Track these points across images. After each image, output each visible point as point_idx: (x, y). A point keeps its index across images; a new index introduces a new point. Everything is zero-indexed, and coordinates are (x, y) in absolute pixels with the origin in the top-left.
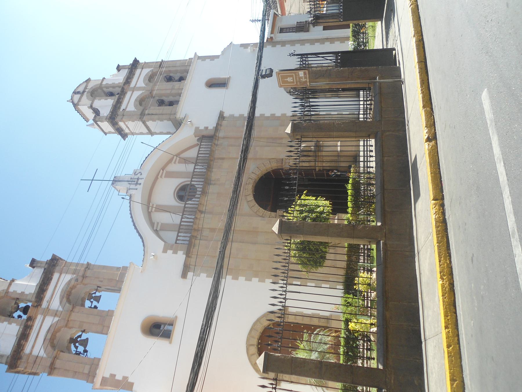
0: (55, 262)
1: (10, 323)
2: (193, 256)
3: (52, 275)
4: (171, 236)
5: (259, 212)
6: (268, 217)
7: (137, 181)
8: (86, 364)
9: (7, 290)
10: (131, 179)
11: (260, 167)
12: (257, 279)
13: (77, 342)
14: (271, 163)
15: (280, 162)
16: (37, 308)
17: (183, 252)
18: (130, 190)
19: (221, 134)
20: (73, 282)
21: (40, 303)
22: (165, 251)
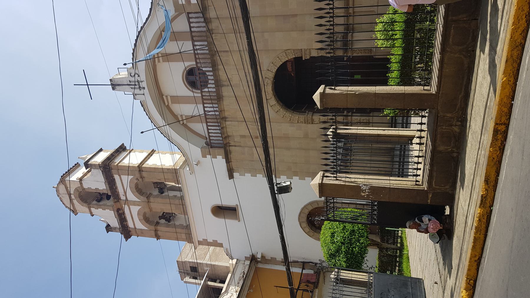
0: (108, 167)
1: (104, 209)
2: (232, 160)
3: (113, 177)
4: (200, 128)
5: (286, 117)
6: (297, 122)
7: (139, 85)
8: (181, 233)
9: (82, 188)
10: (130, 82)
11: (275, 62)
12: (298, 177)
13: (165, 215)
14: (288, 56)
15: (299, 54)
16: (119, 202)
17: (221, 156)
18: (137, 95)
19: (212, 14)
20: (136, 181)
21: (118, 198)
22: (204, 156)
